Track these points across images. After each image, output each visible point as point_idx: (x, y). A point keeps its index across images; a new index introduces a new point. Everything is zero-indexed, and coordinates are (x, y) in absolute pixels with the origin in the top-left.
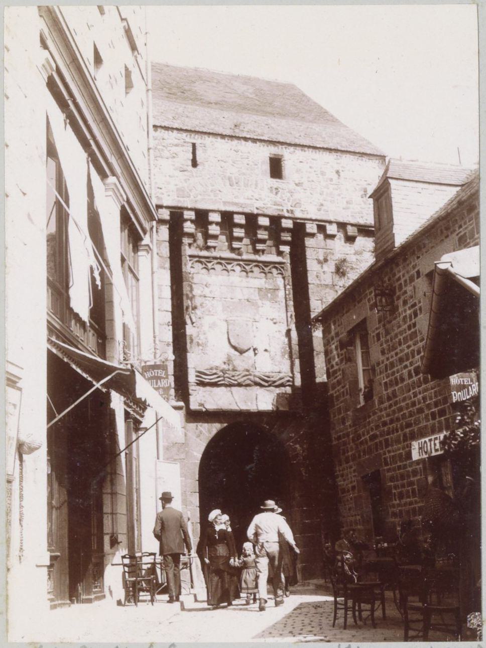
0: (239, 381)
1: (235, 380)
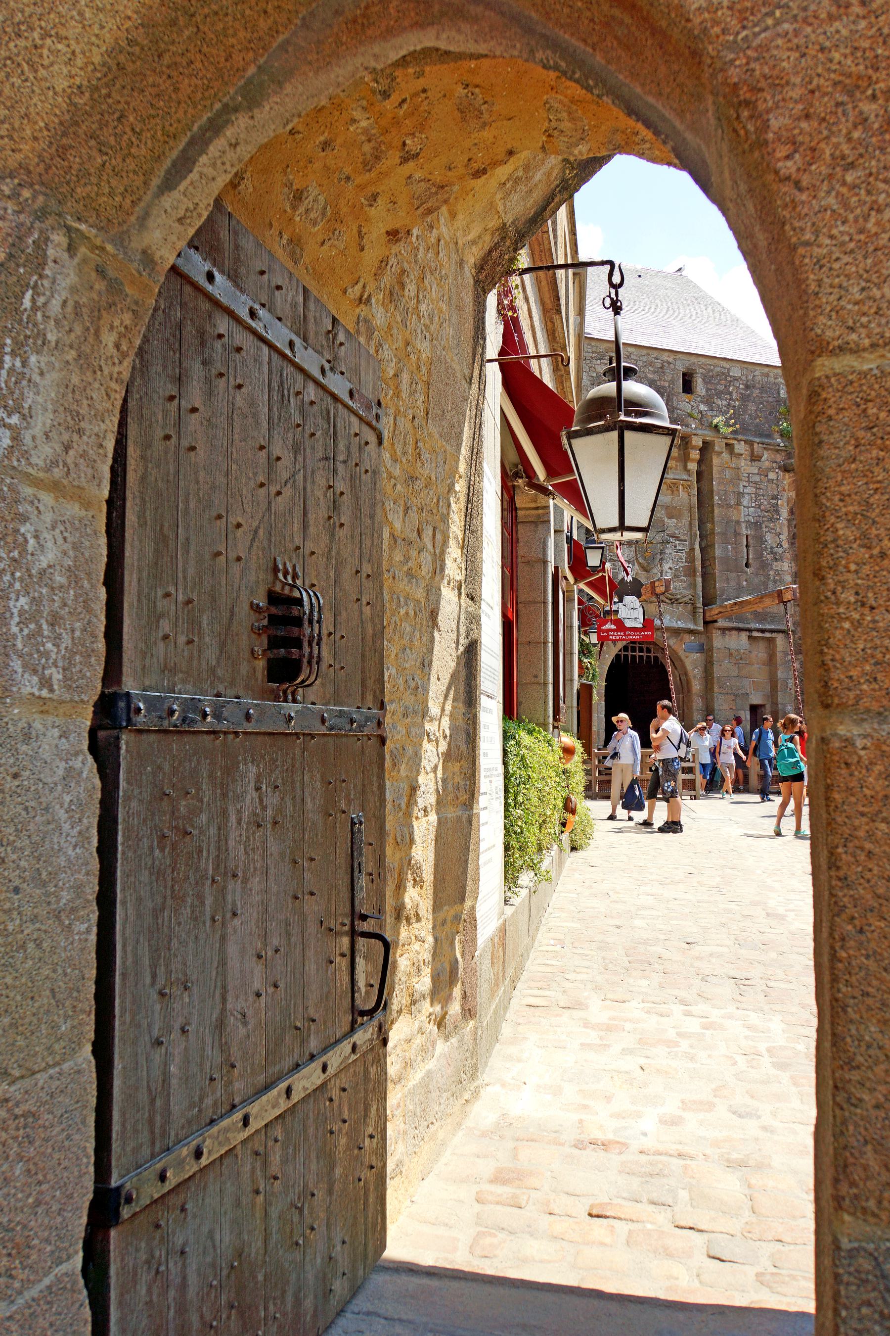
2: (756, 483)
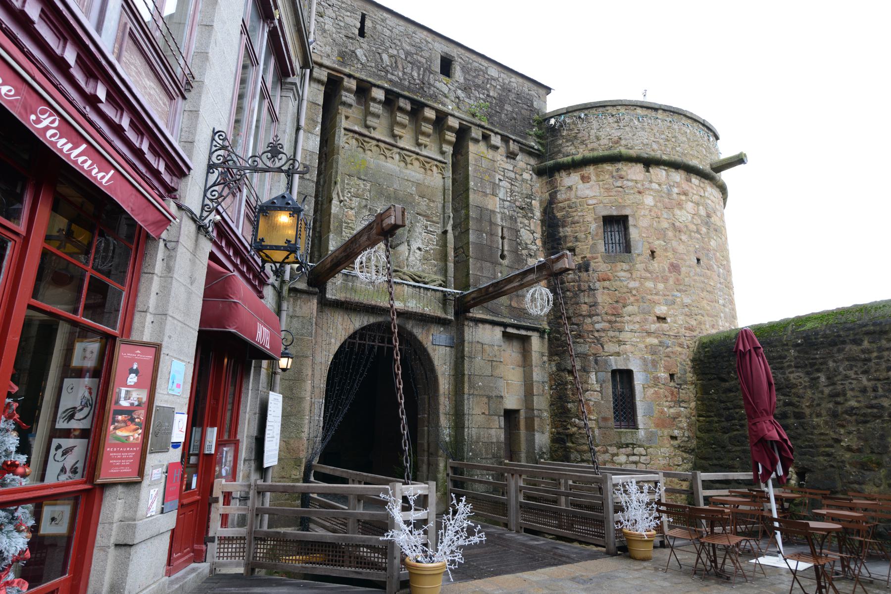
2: (511, 179)
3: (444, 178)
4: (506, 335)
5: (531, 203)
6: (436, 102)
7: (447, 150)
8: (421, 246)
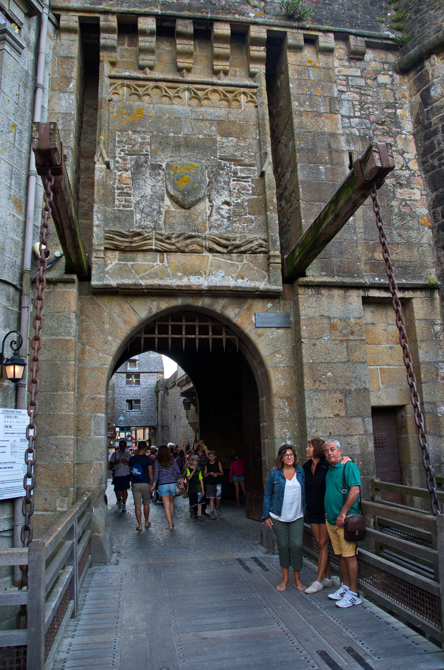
0: (178, 245)
1: (173, 244)
3: (256, 107)
4: (367, 301)
5: (395, 114)
6: (229, 13)
7: (257, 70)
8: (228, 199)
